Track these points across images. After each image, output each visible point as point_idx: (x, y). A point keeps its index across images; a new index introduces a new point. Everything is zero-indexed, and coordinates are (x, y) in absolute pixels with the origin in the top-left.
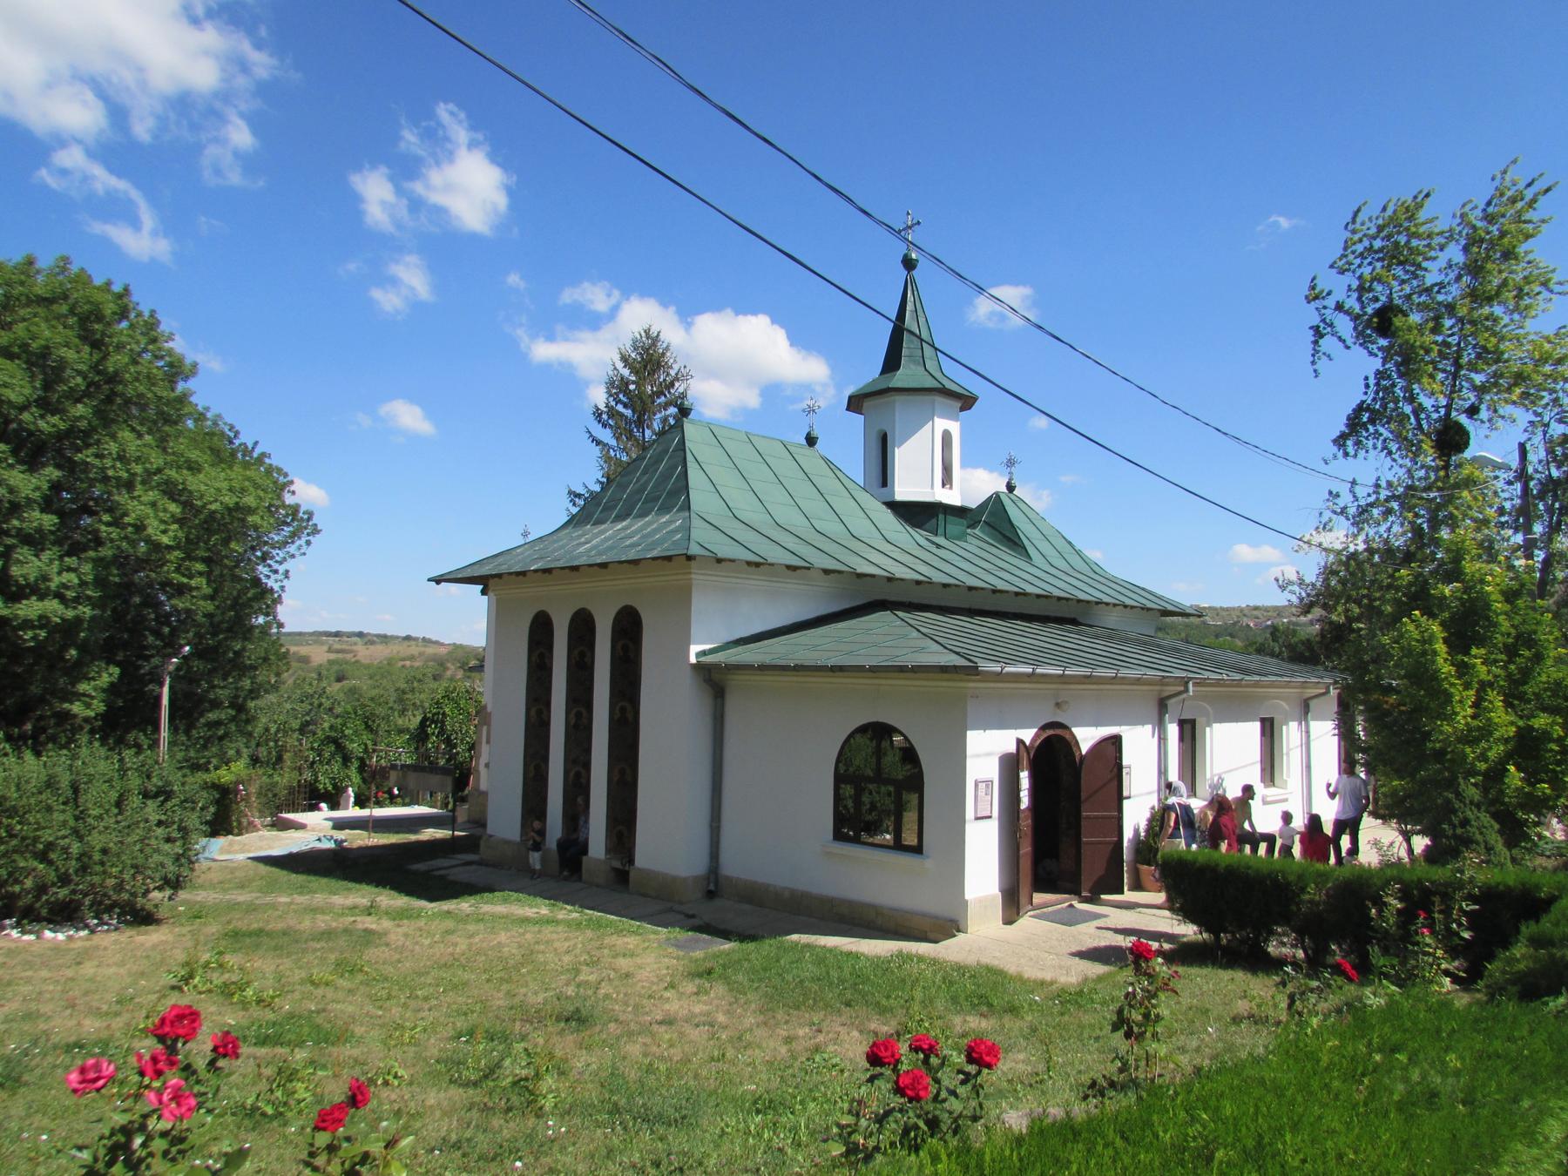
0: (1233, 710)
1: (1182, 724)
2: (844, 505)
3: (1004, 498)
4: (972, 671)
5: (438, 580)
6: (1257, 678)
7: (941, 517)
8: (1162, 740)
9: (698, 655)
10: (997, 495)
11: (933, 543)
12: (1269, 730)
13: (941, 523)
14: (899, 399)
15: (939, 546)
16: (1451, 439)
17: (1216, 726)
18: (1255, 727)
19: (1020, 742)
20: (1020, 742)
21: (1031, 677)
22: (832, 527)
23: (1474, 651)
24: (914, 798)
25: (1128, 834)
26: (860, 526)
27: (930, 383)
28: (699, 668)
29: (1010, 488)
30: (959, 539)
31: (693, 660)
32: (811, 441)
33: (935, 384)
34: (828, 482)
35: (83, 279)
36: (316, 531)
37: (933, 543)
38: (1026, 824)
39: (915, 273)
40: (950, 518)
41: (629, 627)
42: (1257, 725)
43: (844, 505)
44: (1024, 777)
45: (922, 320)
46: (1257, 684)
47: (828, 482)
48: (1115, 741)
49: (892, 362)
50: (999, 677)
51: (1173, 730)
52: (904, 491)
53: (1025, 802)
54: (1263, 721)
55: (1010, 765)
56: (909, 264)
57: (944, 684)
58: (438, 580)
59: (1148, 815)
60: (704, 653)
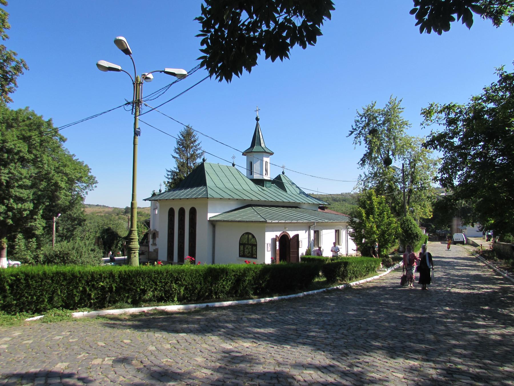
0: (327, 227)
1: (315, 232)
2: (241, 181)
3: (281, 176)
4: (266, 222)
5: (145, 200)
6: (332, 221)
7: (265, 182)
8: (309, 235)
9: (209, 218)
10: (280, 175)
11: (262, 189)
12: (337, 232)
13: (265, 184)
14: (255, 154)
15: (264, 190)
16: (388, 162)
17: (323, 231)
18: (333, 231)
19: (276, 236)
20: (276, 236)
21: (278, 223)
22: (238, 187)
23: (370, 216)
24: (255, 248)
25: (300, 254)
26: (246, 187)
27: (262, 150)
28: (209, 221)
29: (283, 173)
30: (269, 187)
31: (208, 219)
32: (233, 165)
33: (263, 151)
34: (237, 176)
35: (33, 114)
36: (97, 182)
37: (262, 189)
38: (278, 252)
39: (258, 122)
40: (267, 182)
41: (193, 212)
42: (334, 231)
43: (241, 181)
44: (278, 243)
45: (260, 134)
46: (332, 222)
47: (237, 176)
48: (297, 236)
49: (253, 145)
50: (271, 223)
51: (312, 232)
52: (256, 176)
53: (278, 248)
54: (336, 231)
55: (274, 241)
56: (257, 119)
57: (261, 224)
58: (145, 200)
59: (305, 251)
60: (211, 218)
